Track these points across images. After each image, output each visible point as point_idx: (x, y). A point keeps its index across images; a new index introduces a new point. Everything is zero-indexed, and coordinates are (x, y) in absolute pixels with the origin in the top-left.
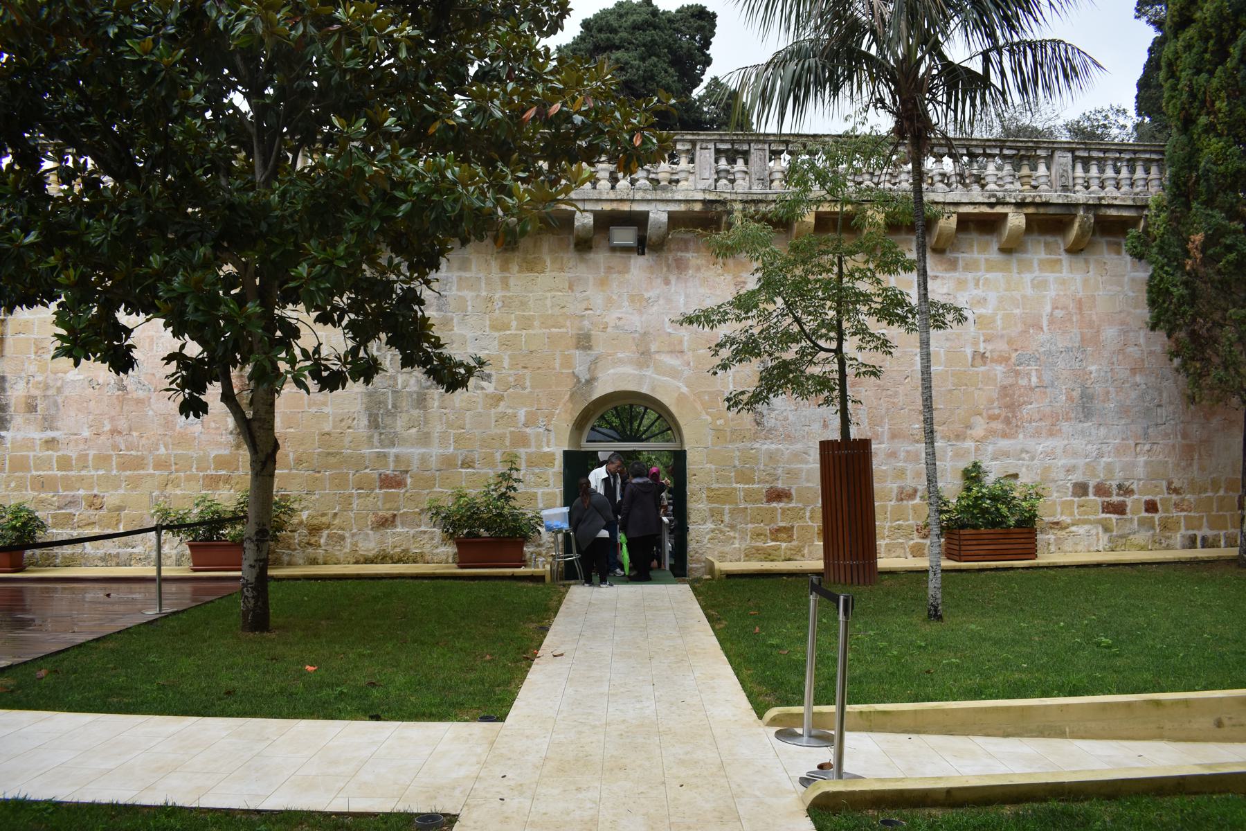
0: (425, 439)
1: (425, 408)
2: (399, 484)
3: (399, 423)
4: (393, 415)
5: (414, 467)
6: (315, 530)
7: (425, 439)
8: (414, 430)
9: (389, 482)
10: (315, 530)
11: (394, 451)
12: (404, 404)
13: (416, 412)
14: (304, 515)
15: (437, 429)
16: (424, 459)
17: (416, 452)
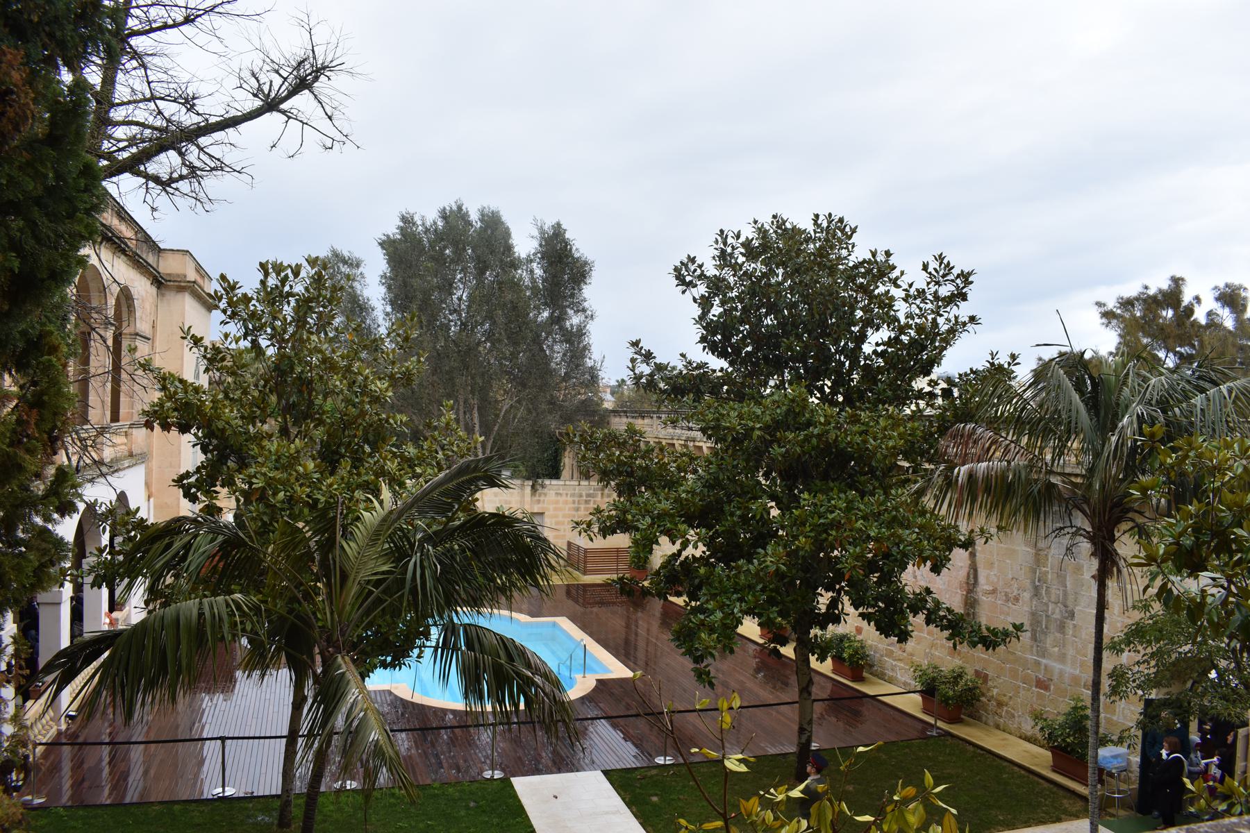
0: (1062, 658)
1: (1064, 633)
2: (1047, 688)
3: (1048, 641)
4: (1045, 634)
5: (1055, 678)
6: (1000, 704)
7: (1062, 658)
8: (1056, 649)
9: (1042, 685)
10: (1000, 704)
11: (1044, 661)
12: (1053, 627)
13: (1058, 635)
14: (995, 691)
15: (1071, 652)
16: (1061, 673)
17: (1057, 666)
